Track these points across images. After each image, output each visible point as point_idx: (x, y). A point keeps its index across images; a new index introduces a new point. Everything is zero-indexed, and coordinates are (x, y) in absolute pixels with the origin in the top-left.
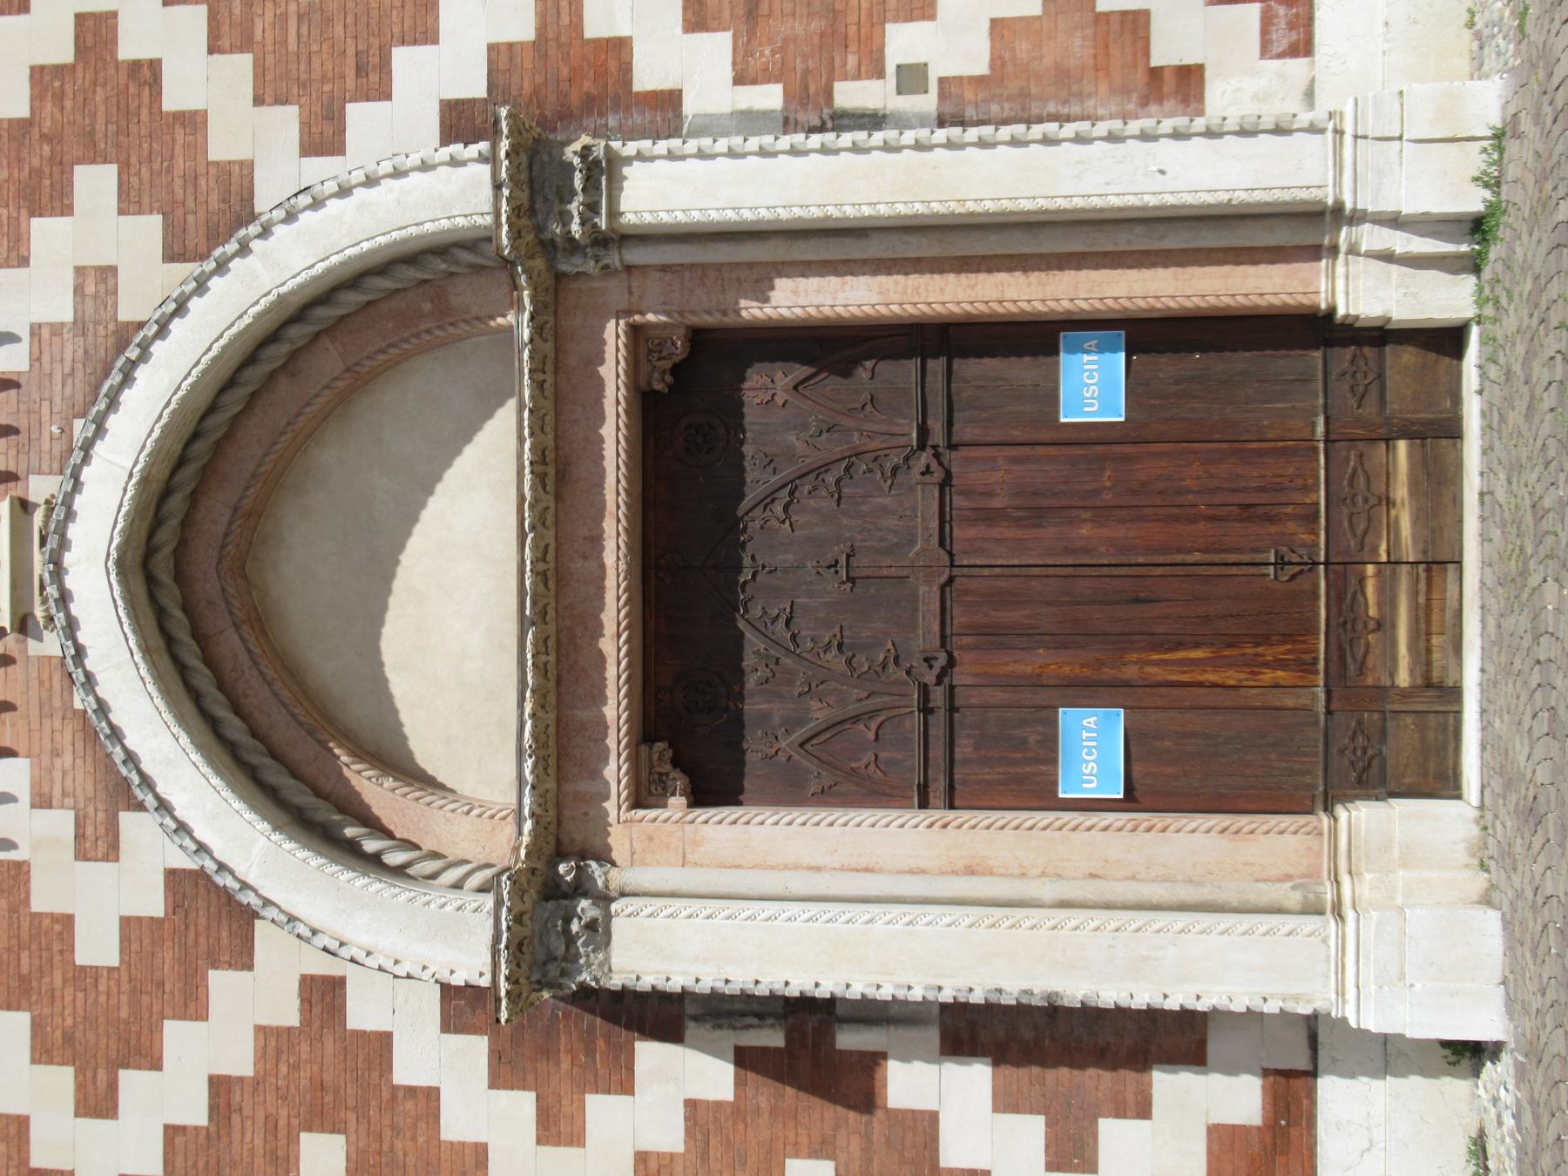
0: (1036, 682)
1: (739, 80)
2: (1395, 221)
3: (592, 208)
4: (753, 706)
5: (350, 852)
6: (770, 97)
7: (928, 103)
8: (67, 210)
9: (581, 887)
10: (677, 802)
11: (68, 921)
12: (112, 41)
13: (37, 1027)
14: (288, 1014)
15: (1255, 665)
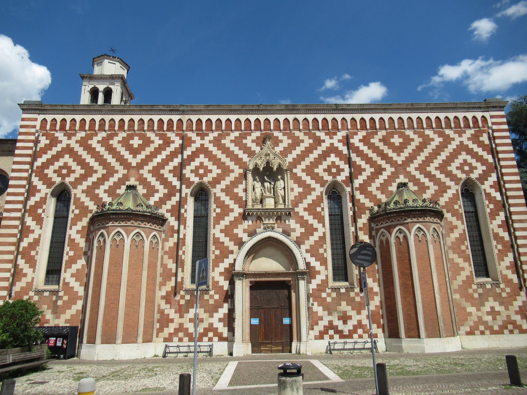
0: (261, 316)
1: (313, 289)
2: (300, 346)
3: (300, 278)
4: (258, 291)
5: (246, 256)
6: (311, 292)
7: (310, 306)
8: (300, 227)
9: (243, 277)
10: (250, 285)
11: (238, 228)
12: (315, 231)
13: (228, 225)
14: (230, 249)
15: (263, 336)
